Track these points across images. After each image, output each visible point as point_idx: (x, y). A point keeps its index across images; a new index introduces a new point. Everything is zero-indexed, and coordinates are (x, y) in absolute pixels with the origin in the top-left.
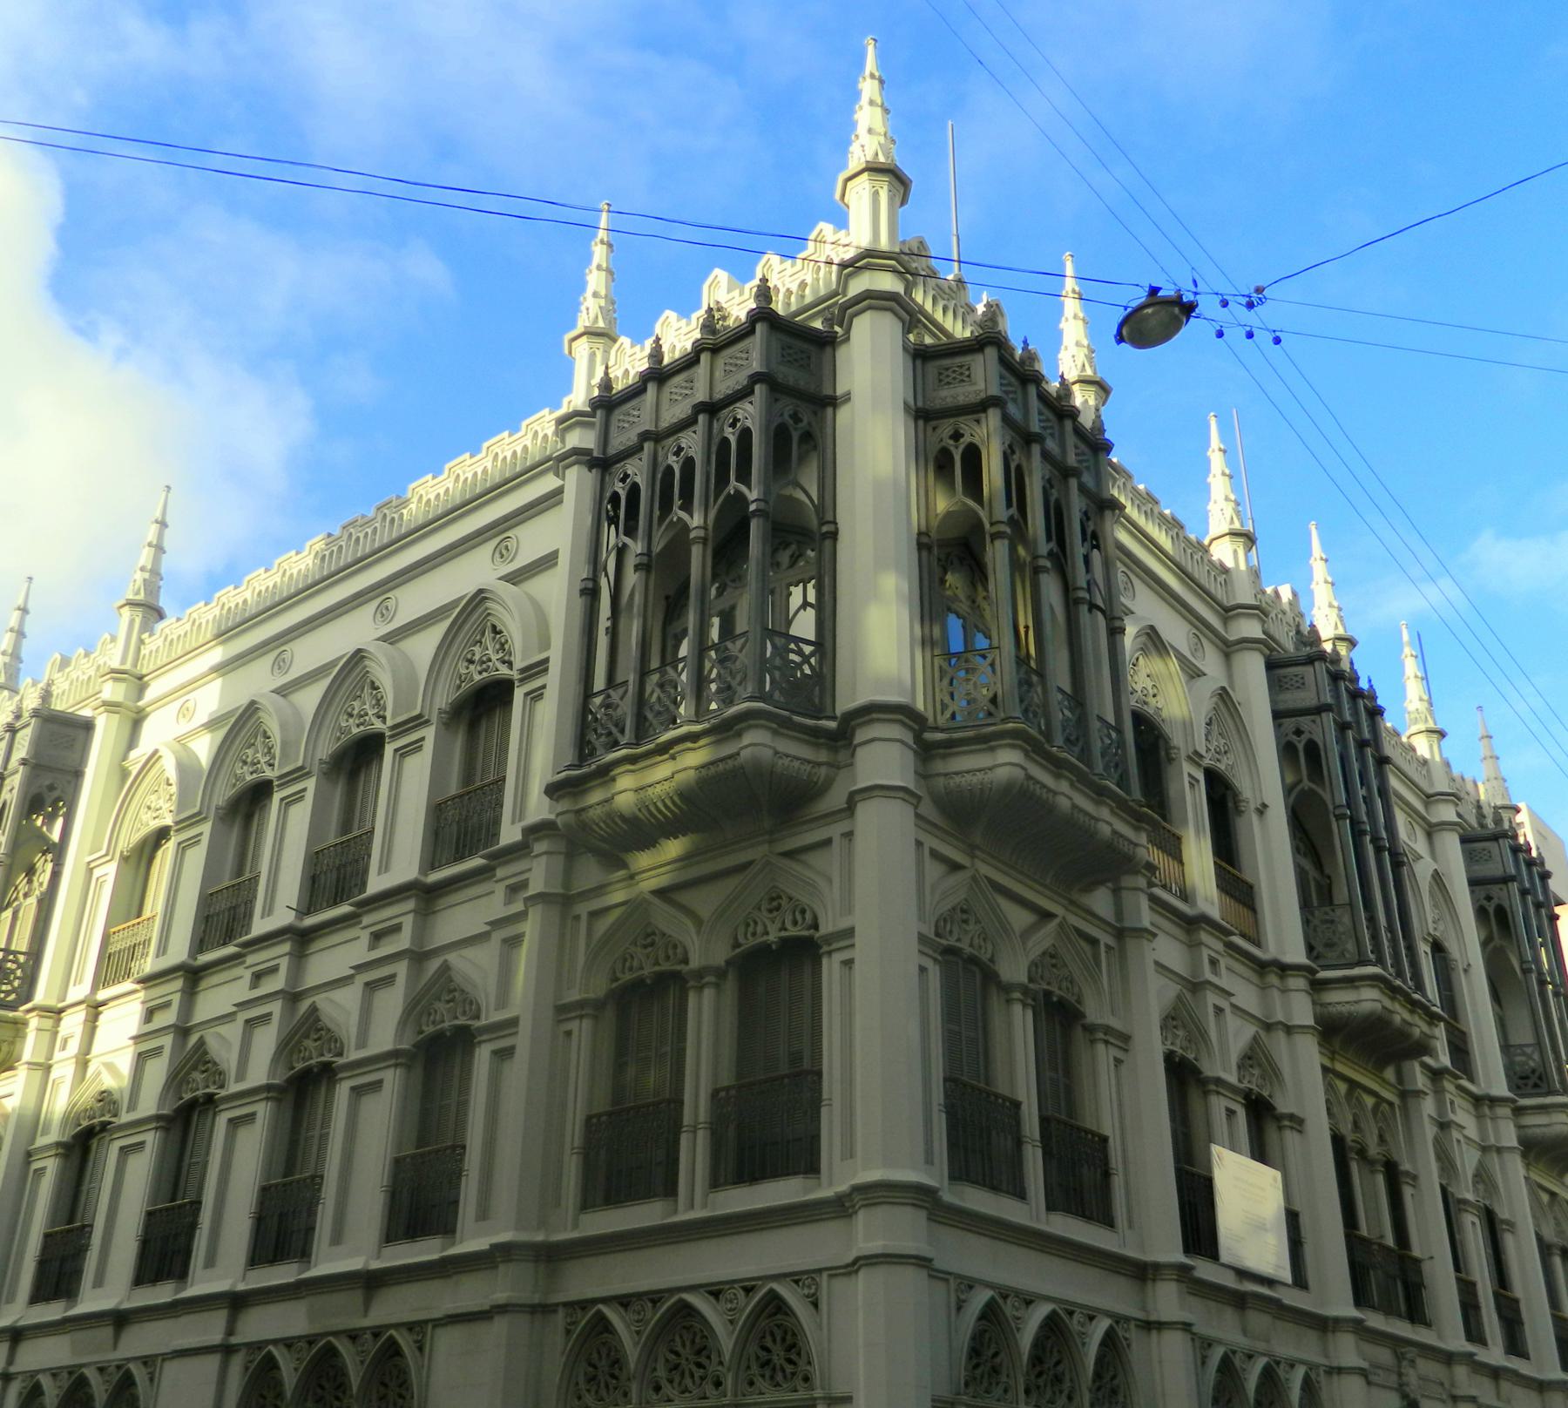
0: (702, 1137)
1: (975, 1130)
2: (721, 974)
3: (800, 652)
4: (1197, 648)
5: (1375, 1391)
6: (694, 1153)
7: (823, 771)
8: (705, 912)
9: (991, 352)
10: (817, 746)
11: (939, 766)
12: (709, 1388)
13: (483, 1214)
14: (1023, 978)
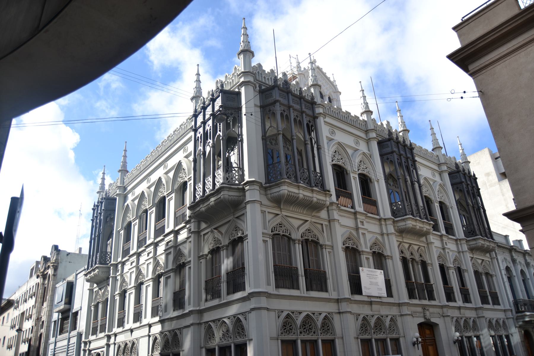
0: (225, 284)
1: (284, 276)
2: (227, 246)
3: (235, 170)
4: (357, 143)
5: (415, 318)
6: (224, 287)
7: (241, 197)
8: (223, 232)
9: (276, 89)
10: (240, 192)
11: (269, 192)
12: (229, 339)
13: (189, 304)
14: (299, 237)
